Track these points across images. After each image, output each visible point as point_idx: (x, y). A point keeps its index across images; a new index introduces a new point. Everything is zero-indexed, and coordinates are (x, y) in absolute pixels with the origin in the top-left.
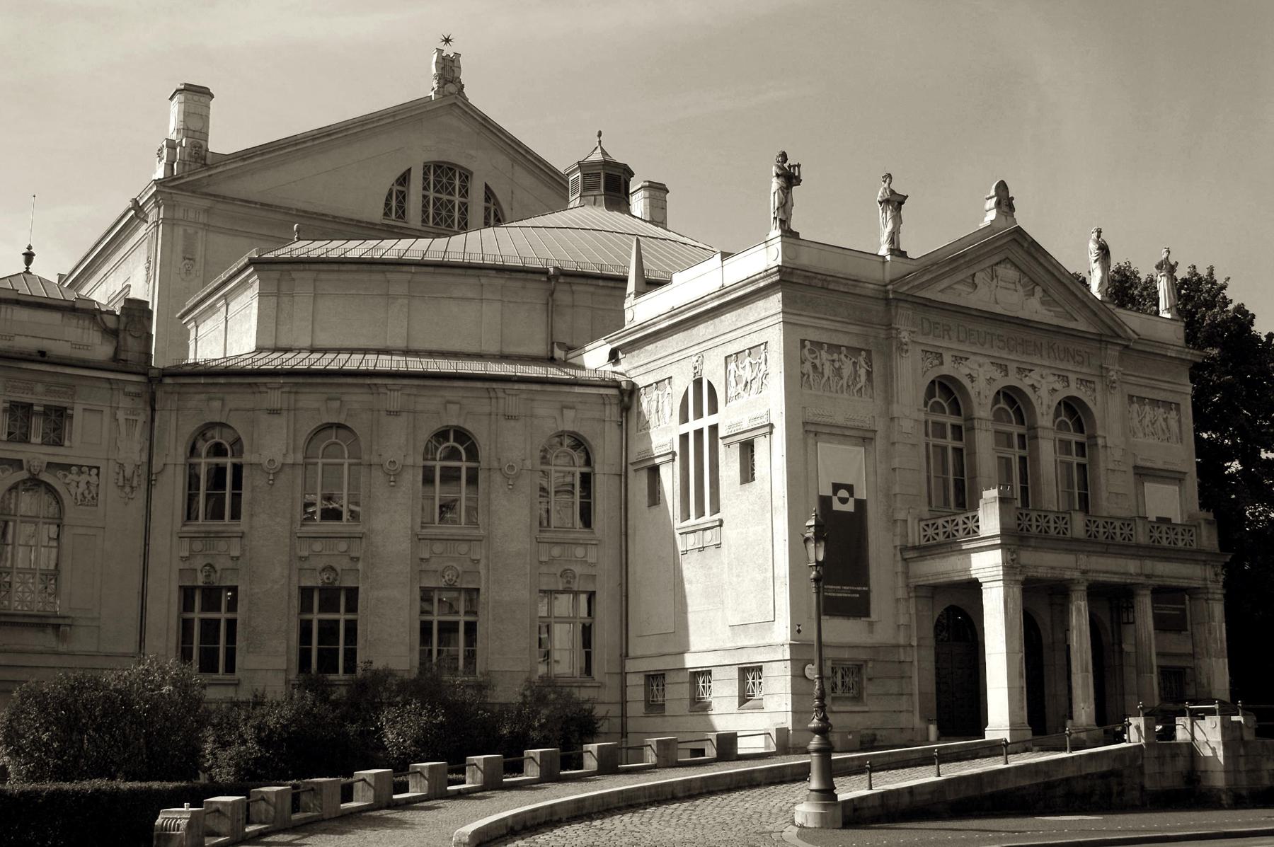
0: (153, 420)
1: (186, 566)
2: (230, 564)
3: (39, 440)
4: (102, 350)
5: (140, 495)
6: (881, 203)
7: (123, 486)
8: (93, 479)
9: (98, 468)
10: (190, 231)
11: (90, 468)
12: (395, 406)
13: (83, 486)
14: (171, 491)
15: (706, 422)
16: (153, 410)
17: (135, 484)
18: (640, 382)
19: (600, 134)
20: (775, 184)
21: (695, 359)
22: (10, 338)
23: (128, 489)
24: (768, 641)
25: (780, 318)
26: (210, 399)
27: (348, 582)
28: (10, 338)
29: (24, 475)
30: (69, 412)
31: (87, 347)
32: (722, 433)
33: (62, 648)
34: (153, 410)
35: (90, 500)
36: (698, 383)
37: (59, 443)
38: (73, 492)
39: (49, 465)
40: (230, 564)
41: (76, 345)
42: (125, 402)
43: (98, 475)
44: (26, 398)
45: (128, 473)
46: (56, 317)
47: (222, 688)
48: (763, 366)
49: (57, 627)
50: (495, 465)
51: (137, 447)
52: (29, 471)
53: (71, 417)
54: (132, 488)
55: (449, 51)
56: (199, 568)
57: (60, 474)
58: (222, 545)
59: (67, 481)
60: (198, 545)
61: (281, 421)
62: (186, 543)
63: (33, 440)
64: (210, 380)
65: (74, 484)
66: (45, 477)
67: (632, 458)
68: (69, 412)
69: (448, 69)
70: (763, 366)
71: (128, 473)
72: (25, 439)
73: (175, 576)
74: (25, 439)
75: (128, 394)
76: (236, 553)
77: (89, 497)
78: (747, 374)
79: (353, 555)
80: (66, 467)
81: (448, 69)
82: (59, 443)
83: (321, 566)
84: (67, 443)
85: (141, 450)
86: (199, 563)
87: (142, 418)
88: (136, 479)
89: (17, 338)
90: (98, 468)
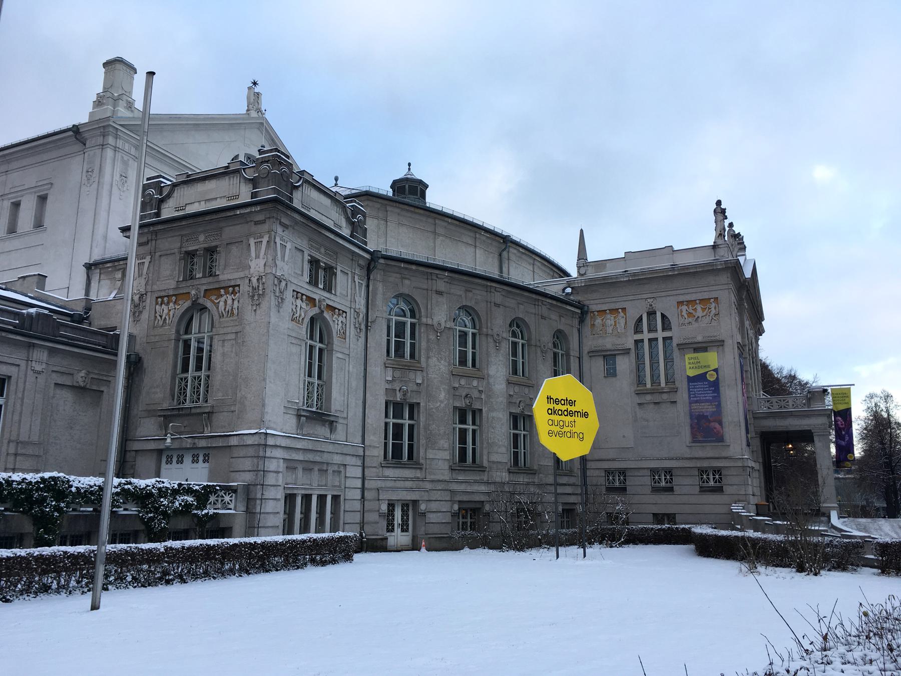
0: (368, 286)
2: (415, 388)
5: (363, 335)
10: (126, 158)
12: (498, 301)
14: (379, 337)
15: (660, 334)
16: (369, 279)
18: (594, 308)
19: (409, 164)
24: (724, 454)
26: (403, 278)
27: (476, 406)
28: (309, 209)
31: (340, 227)
32: (675, 342)
34: (369, 279)
35: (343, 335)
36: (651, 314)
40: (415, 388)
44: (318, 256)
46: (327, 201)
47: (414, 471)
48: (713, 309)
49: (331, 423)
50: (538, 344)
55: (256, 90)
57: (331, 313)
58: (412, 375)
60: (398, 374)
61: (442, 299)
62: (390, 372)
64: (407, 266)
67: (586, 350)
69: (254, 98)
70: (713, 309)
73: (383, 392)
75: (359, 265)
76: (419, 381)
79: (481, 389)
81: (254, 98)
83: (464, 394)
87: (364, 283)
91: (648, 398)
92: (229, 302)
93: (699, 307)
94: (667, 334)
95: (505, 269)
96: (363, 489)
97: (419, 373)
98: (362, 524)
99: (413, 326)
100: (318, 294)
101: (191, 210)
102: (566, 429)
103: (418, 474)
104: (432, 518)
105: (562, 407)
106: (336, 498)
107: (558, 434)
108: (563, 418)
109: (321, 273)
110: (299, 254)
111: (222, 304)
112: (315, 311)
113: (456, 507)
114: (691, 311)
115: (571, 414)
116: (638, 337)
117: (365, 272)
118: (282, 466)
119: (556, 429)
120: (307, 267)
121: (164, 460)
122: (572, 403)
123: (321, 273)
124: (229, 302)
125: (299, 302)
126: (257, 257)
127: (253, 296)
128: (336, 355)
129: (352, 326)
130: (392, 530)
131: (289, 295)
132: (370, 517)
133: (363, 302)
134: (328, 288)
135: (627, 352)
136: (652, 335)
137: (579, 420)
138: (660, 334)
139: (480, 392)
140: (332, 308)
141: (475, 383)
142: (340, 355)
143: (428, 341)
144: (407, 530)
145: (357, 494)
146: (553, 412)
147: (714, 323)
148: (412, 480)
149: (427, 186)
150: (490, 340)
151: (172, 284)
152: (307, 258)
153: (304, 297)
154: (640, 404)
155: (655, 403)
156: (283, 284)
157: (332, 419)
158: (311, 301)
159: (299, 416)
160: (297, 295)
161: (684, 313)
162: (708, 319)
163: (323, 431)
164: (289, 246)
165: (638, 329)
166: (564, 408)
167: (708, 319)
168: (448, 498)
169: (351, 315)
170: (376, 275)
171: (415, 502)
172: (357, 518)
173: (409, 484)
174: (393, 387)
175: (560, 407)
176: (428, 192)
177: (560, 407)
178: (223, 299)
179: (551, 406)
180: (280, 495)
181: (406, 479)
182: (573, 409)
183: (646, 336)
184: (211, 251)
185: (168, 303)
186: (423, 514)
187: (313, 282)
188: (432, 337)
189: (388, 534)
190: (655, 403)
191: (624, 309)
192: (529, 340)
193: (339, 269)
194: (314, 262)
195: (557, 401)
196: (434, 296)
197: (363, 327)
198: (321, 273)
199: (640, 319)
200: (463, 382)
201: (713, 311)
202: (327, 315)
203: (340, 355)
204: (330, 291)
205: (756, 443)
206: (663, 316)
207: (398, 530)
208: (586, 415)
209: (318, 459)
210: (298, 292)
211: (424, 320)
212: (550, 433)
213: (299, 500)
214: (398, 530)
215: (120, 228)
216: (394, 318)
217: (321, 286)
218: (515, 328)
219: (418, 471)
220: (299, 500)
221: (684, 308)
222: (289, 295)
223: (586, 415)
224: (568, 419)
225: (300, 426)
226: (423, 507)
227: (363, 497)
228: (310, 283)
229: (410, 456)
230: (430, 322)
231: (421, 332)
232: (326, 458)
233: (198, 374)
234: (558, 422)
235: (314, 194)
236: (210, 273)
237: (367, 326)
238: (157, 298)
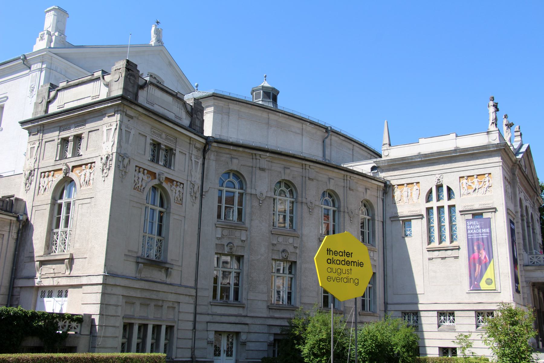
1: (218, 242)
2: (240, 243)
3: (162, 164)
4: (186, 122)
6: (506, 125)
9: (183, 184)
11: (181, 183)
14: (211, 203)
16: (204, 158)
20: (492, 109)
21: (439, 176)
22: (153, 105)
25: (501, 164)
28: (153, 105)
31: (180, 119)
32: (458, 209)
33: (168, 281)
34: (204, 158)
35: (180, 201)
36: (439, 187)
40: (240, 243)
41: (176, 116)
42: (195, 152)
44: (159, 140)
47: (237, 309)
48: (487, 183)
49: (167, 269)
52: (159, 180)
56: (226, 244)
57: (169, 184)
58: (237, 233)
60: (226, 232)
61: (265, 174)
62: (219, 230)
63: (160, 163)
64: (235, 148)
70: (487, 183)
74: (157, 162)
75: (196, 148)
77: (179, 199)
78: (476, 185)
79: (295, 245)
83: (281, 249)
84: (172, 168)
86: (225, 242)
87: (200, 161)
89: (155, 106)
90: (183, 184)
91: (436, 254)
92: (88, 174)
93: (476, 180)
94: (451, 203)
95: (327, 153)
96: (195, 322)
97: (243, 232)
98: (193, 349)
99: (241, 195)
100: (158, 169)
101: (67, 107)
102: (343, 276)
103: (241, 311)
104: (251, 346)
105: (339, 259)
106: (170, 328)
107: (337, 280)
108: (341, 266)
109: (162, 154)
110: (143, 139)
111: (83, 177)
112: (156, 182)
113: (272, 338)
114: (471, 184)
115: (348, 263)
116: (429, 205)
117: (200, 154)
118: (121, 301)
119: (334, 275)
120: (149, 148)
121: (40, 294)
122: (349, 254)
123: (161, 152)
124: (88, 174)
125: (141, 175)
126: (108, 140)
127: (103, 170)
128: (172, 217)
129: (188, 195)
130: (219, 355)
131: (131, 169)
132: (199, 344)
133: (199, 176)
134: (168, 164)
135: (421, 217)
136: (440, 204)
137: (355, 269)
138: (445, 202)
139: (295, 248)
140: (171, 181)
141: (291, 240)
142: (176, 217)
143: (252, 207)
144: (231, 355)
145: (190, 326)
146: (330, 261)
147: (488, 193)
148: (236, 316)
149: (278, 92)
150: (305, 207)
151: (52, 162)
152: (149, 141)
153: (146, 171)
154: (430, 259)
155: (443, 258)
156: (126, 161)
157: (167, 266)
158: (153, 175)
159: (138, 263)
160: (139, 169)
161: (464, 185)
162: (483, 190)
163: (158, 275)
164: (133, 132)
165: (429, 198)
166: (342, 258)
167: (483, 190)
168: (266, 331)
169: (187, 187)
170: (211, 156)
171: (238, 334)
172: (189, 344)
173: (232, 319)
174: (222, 243)
175: (338, 257)
176: (279, 97)
177: (338, 257)
178: (83, 173)
179: (330, 257)
180: (120, 323)
181: (277, 318)
182: (350, 259)
183: (434, 204)
184: (78, 138)
185: (48, 176)
186: (244, 344)
187: (155, 159)
188: (255, 203)
189: (216, 358)
190: (443, 258)
191: (418, 183)
192: (339, 208)
193: (178, 150)
194: (156, 146)
195: (336, 253)
196: (258, 171)
197: (198, 195)
198: (162, 154)
199: (430, 192)
200: (281, 239)
201: (487, 184)
202: (165, 185)
203: (176, 217)
204: (170, 167)
205: (527, 291)
206: (449, 189)
207: (223, 355)
208: (361, 264)
209: (154, 297)
210: (140, 168)
211: (249, 191)
212: (329, 279)
213: (136, 329)
214: (223, 355)
215: (23, 123)
216: (225, 189)
217: (162, 163)
218: (327, 198)
219: (241, 309)
220: (136, 329)
221: (464, 181)
222: (131, 169)
223: (361, 264)
224: (346, 267)
225: (139, 271)
226: (243, 337)
227: (195, 328)
228: (152, 161)
229: (236, 298)
230: (253, 192)
231: (247, 200)
232: (161, 296)
233: (66, 229)
234: (336, 270)
235: (159, 93)
236: (76, 153)
237: (202, 195)
238: (41, 173)
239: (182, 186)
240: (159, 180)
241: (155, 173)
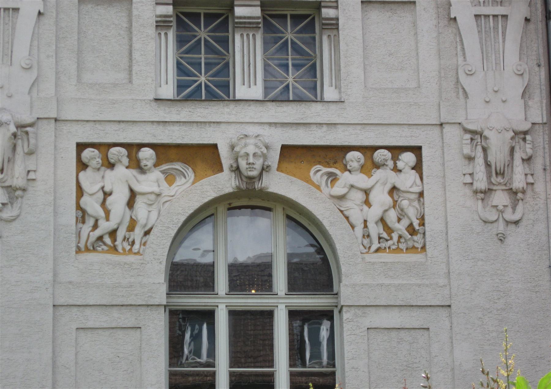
3: (257, 92)
7: (487, 192)
8: (408, 180)
9: (417, 150)
11: (396, 151)
13: (381, 198)
17: (518, 182)
23: (500, 198)
29: (224, 183)
30: (327, 12)
37: (312, 93)
38: (356, 216)
39: (287, 151)
43: (418, 167)
45: (498, 156)
51: (514, 87)
52: (237, 170)
53: (333, 25)
54: (513, 192)
57: (318, 172)
59: (338, 189)
63: (241, 91)
65: (359, 196)
66: (279, 184)
68: (327, 12)
71: (498, 156)
72: (220, 91)
74: (220, 91)
77: (401, 227)
80: (333, 155)
82: (312, 93)
84: (330, 93)
85: (525, 94)
88: (519, 168)
90: (417, 150)
153: (146, 154)
158: (204, 156)
169: (445, 154)
210: (103, 147)
239: (408, 158)
240: (237, 170)
241: (215, 147)
